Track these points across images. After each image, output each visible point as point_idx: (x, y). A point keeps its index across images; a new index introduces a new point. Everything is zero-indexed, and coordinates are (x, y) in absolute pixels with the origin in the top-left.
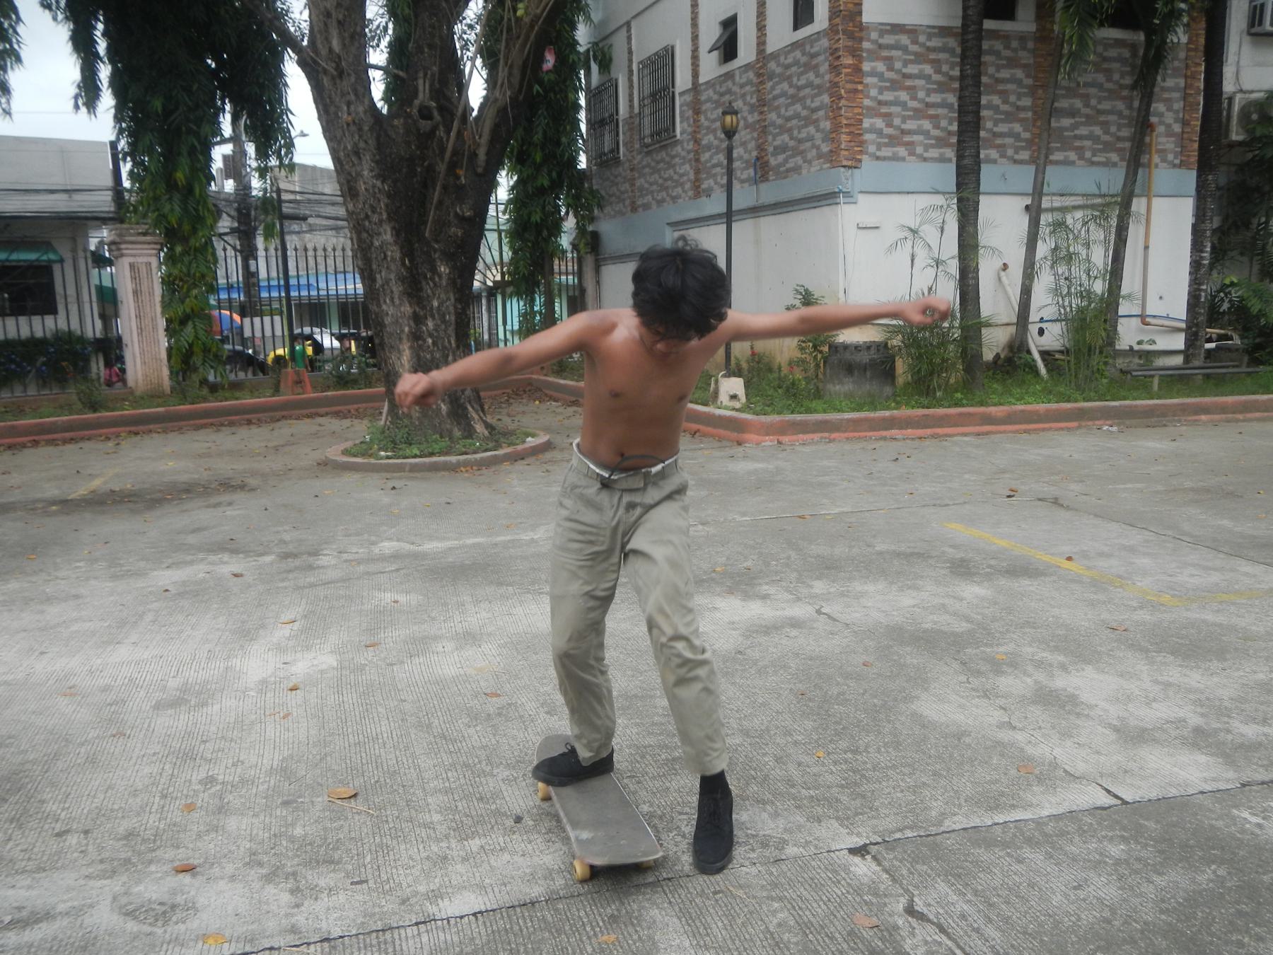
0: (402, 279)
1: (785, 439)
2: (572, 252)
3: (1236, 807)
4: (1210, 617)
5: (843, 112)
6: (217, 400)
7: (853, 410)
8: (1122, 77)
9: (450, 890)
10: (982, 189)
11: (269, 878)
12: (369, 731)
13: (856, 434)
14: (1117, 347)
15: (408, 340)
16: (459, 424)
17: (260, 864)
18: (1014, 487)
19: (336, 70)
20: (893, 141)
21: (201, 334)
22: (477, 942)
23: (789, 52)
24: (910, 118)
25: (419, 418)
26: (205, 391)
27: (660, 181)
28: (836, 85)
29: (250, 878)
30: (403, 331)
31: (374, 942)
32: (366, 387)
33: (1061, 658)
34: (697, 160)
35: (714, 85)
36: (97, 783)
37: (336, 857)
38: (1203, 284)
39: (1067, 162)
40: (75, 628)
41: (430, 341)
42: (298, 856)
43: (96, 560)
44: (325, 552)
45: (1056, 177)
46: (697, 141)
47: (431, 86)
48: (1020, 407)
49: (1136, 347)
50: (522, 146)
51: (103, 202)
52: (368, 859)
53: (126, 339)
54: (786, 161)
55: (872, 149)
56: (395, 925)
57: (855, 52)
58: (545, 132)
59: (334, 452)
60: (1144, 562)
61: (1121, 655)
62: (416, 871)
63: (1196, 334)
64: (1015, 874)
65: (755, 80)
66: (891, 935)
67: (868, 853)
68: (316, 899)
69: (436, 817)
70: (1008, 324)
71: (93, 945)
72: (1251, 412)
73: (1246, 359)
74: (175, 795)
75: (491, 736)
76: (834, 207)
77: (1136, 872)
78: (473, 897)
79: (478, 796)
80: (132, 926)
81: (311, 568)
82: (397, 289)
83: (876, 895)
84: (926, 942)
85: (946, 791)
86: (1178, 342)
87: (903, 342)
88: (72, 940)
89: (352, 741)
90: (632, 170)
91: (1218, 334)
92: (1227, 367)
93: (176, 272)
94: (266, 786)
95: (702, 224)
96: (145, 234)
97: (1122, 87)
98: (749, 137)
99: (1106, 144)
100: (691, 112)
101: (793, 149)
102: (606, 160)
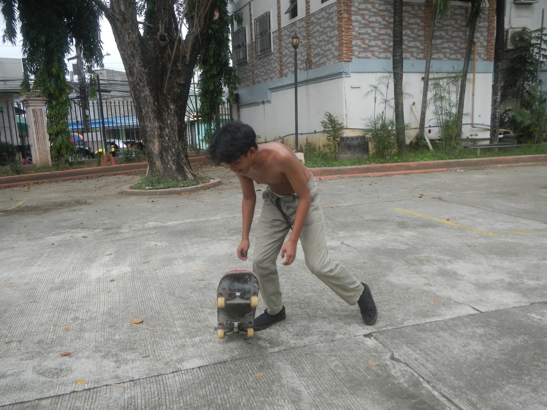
0: (154, 111)
1: (323, 178)
2: (227, 103)
3: (530, 312)
5: (344, 38)
6: (73, 169)
7: (351, 165)
8: (462, 22)
9: (187, 358)
10: (404, 70)
11: (104, 357)
12: (147, 296)
13: (353, 175)
14: (462, 137)
16: (180, 174)
17: (101, 351)
18: (422, 194)
19: (123, 19)
20: (365, 50)
21: (65, 139)
22: (201, 378)
23: (320, 12)
24: (372, 40)
25: (163, 172)
26: (67, 165)
27: (265, 71)
28: (340, 26)
29: (96, 357)
30: (155, 134)
31: (154, 380)
33: (448, 258)
34: (281, 61)
35: (288, 28)
36: (24, 321)
37: (135, 347)
38: (497, 109)
39: (439, 59)
40: (12, 260)
41: (167, 138)
42: (117, 347)
43: (21, 233)
44: (123, 227)
45: (435, 65)
46: (280, 53)
47: (165, 26)
49: (470, 137)
50: (204, 57)
52: (149, 347)
54: (320, 60)
55: (356, 53)
56: (163, 373)
57: (348, 12)
58: (214, 51)
60: (480, 220)
62: (171, 351)
64: (437, 342)
65: (305, 25)
66: (385, 368)
67: (372, 336)
68: (127, 364)
69: (179, 329)
70: (415, 128)
71: (25, 387)
72: (519, 162)
73: (516, 141)
75: (202, 296)
76: (341, 79)
77: (489, 339)
78: (198, 360)
79: (197, 320)
80: (42, 379)
81: (117, 233)
82: (152, 115)
83: (377, 352)
84: (401, 371)
85: (404, 310)
86: (487, 135)
87: (372, 136)
88: (15, 386)
89: (139, 300)
90: (252, 66)
93: (53, 113)
94: (101, 320)
95: (283, 89)
96: (39, 96)
97: (462, 26)
98: (303, 50)
99: (455, 50)
100: (277, 40)
101: (322, 54)
102: (241, 63)
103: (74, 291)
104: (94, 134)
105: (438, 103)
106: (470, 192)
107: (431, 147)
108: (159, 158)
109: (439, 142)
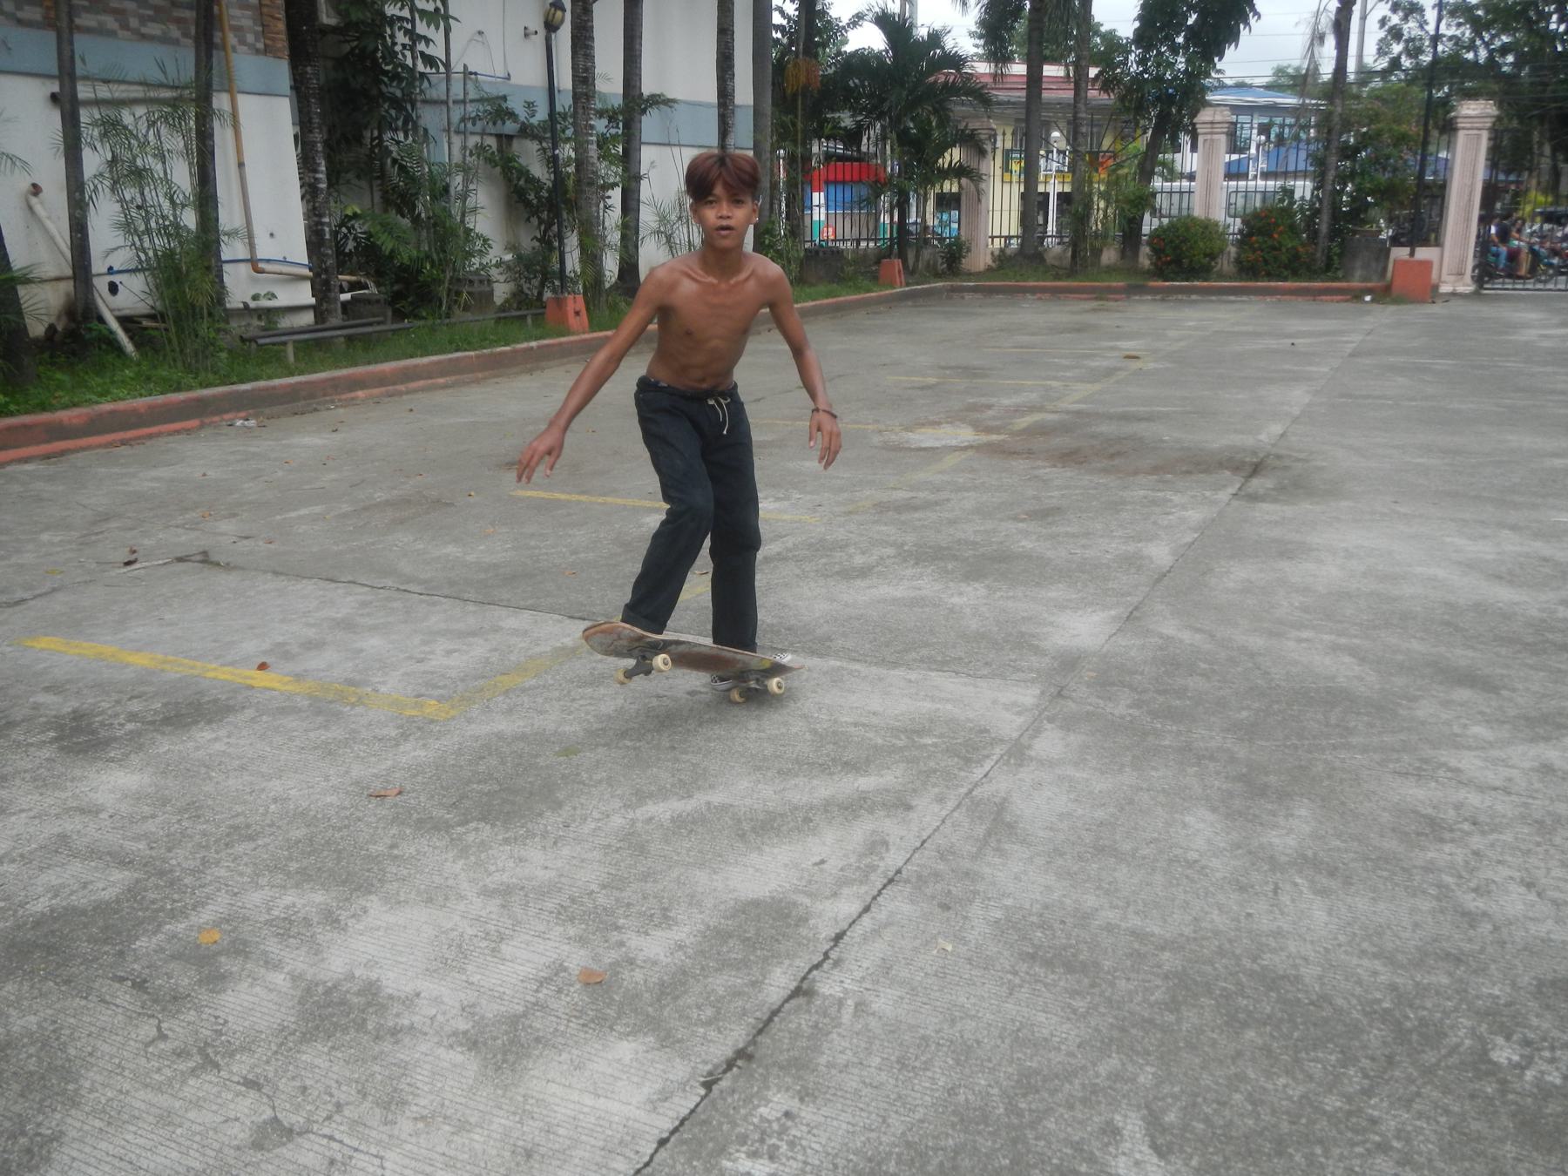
4: (503, 725)
14: (228, 306)
33: (319, 897)
39: (101, 31)
48: (107, 407)
49: (253, 304)
60: (373, 643)
61: (412, 850)
63: (327, 283)
70: (58, 279)
73: (390, 313)
86: (303, 295)
91: (349, 282)
92: (370, 324)
105: (130, 193)
106: (303, 512)
107: (129, 347)
109: (154, 324)
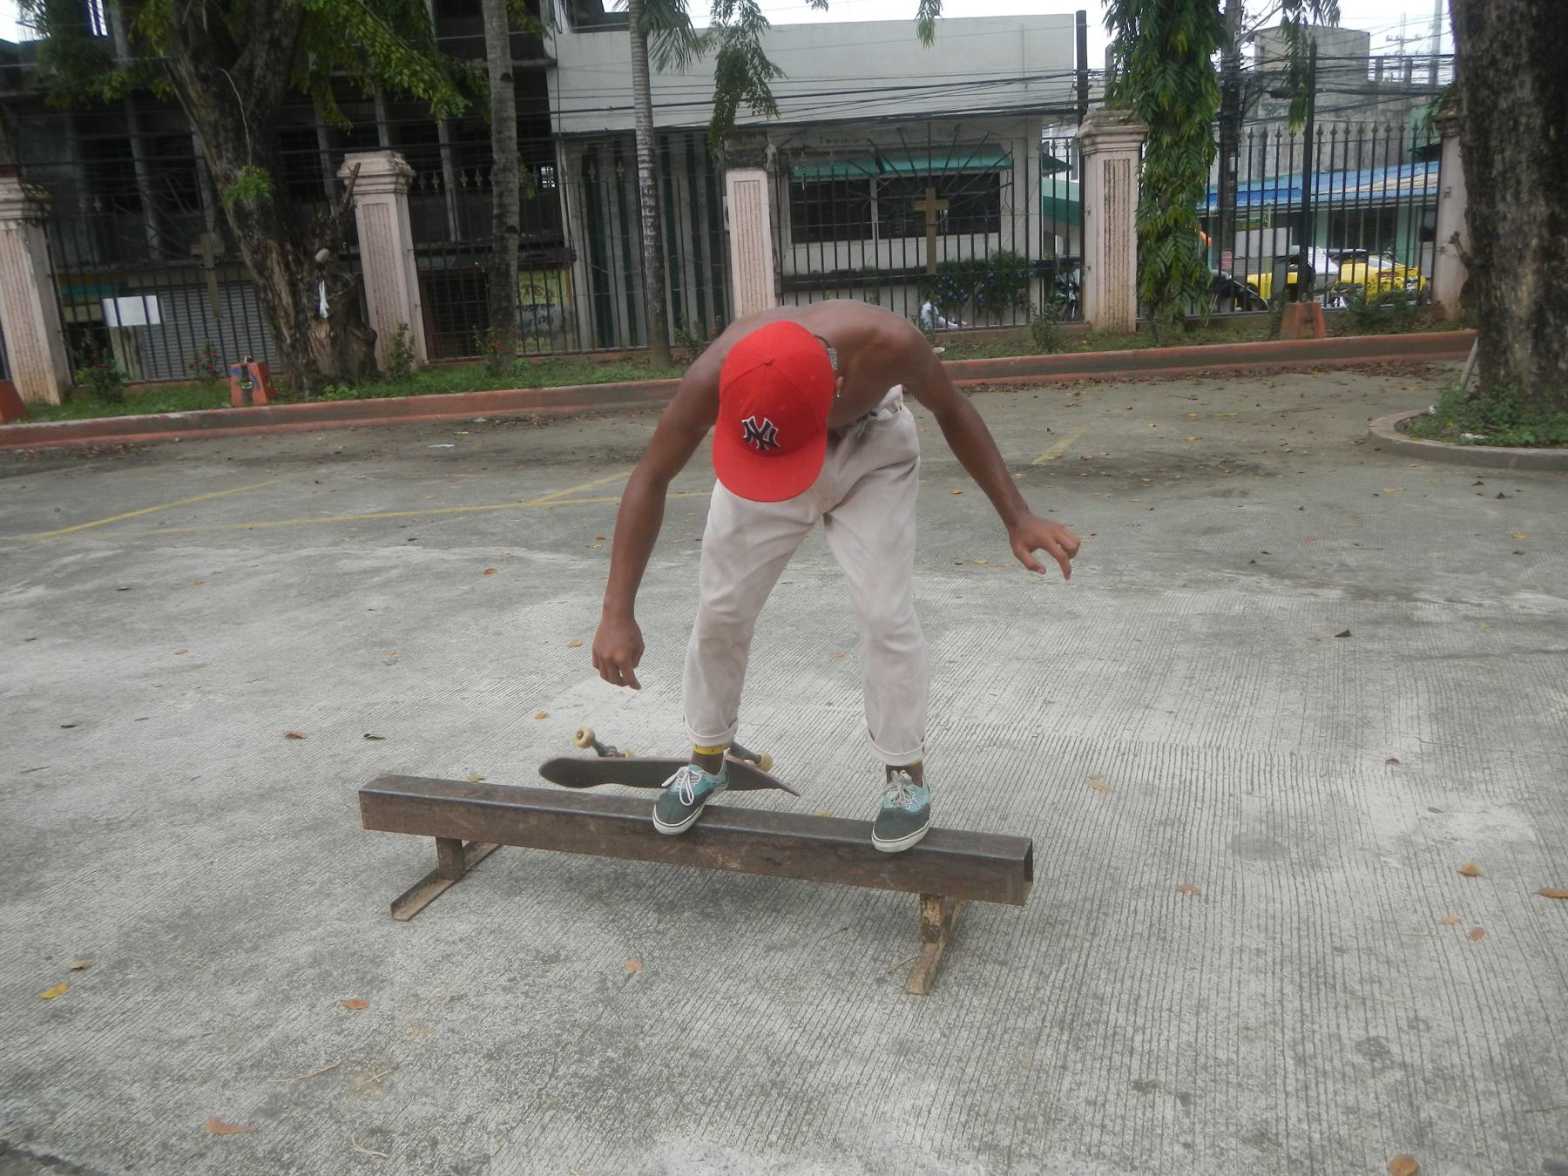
0: (1537, 161)
6: (1194, 341)
15: (1534, 260)
21: (1183, 252)
25: (1533, 385)
26: (1179, 329)
30: (1527, 245)
32: (1403, 331)
36: (1178, 987)
40: (1081, 666)
44: (1427, 596)
51: (1062, 91)
53: (1090, 258)
59: (1383, 426)
74: (1320, 1060)
81: (1408, 622)
82: (1527, 177)
93: (1159, 170)
96: (1126, 122)
103: (1328, 884)
104: (1268, 232)
108: (1528, 334)
